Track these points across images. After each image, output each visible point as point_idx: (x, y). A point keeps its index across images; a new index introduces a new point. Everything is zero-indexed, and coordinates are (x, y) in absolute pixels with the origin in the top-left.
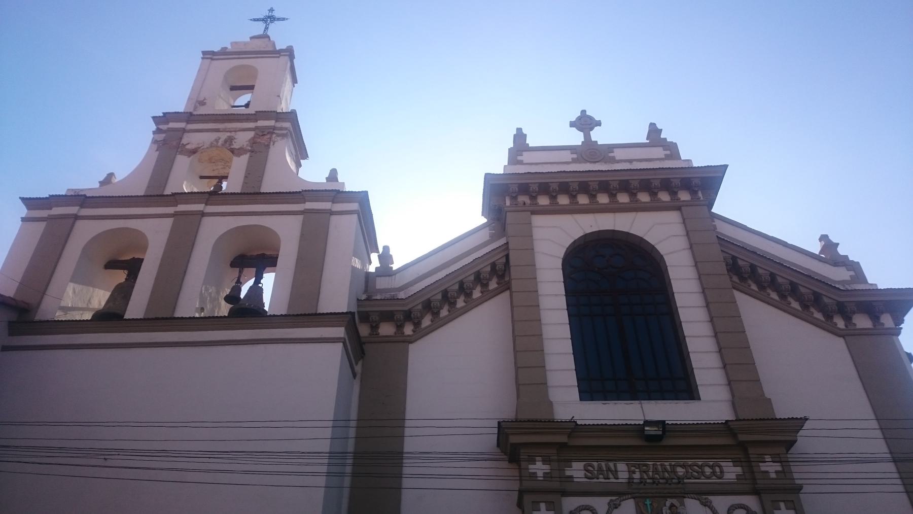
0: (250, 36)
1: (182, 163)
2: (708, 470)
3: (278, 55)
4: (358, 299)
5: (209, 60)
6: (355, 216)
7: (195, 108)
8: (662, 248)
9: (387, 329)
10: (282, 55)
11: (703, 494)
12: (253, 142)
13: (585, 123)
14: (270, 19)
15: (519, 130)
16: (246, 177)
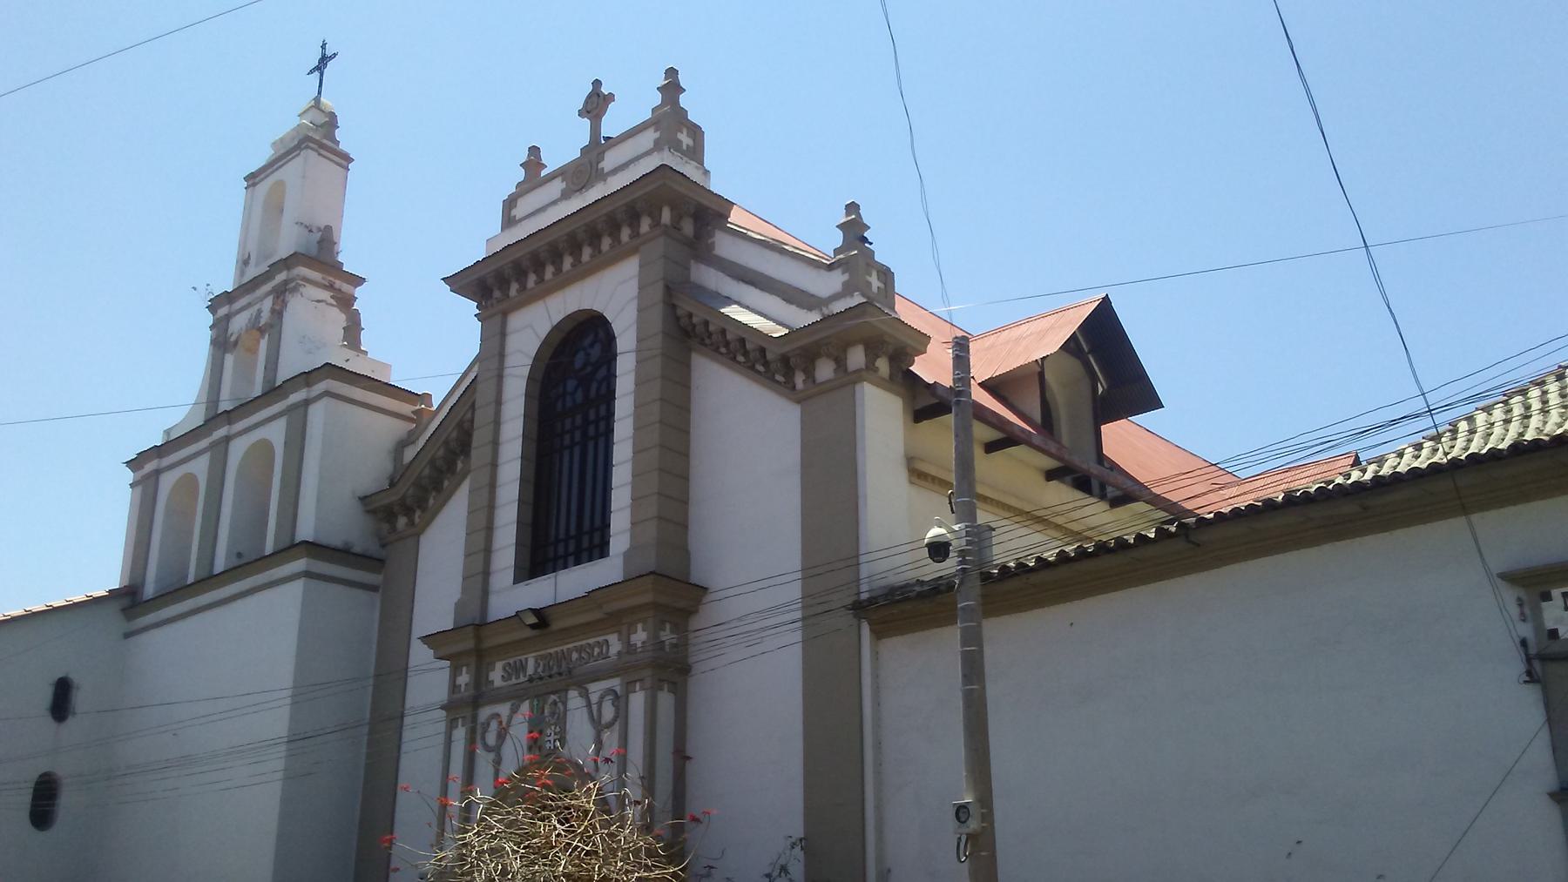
0: (299, 113)
1: (229, 360)
2: (597, 650)
3: (298, 152)
4: (360, 498)
5: (251, 188)
6: (325, 400)
7: (242, 273)
8: (617, 328)
9: (402, 522)
10: (303, 149)
11: (582, 685)
12: (273, 311)
13: (596, 103)
14: (324, 60)
15: (534, 151)
16: (265, 368)
